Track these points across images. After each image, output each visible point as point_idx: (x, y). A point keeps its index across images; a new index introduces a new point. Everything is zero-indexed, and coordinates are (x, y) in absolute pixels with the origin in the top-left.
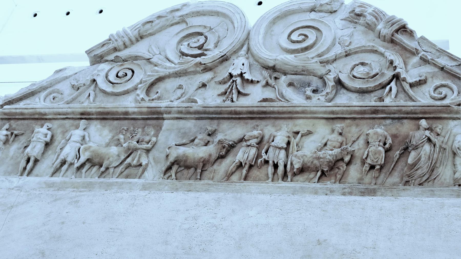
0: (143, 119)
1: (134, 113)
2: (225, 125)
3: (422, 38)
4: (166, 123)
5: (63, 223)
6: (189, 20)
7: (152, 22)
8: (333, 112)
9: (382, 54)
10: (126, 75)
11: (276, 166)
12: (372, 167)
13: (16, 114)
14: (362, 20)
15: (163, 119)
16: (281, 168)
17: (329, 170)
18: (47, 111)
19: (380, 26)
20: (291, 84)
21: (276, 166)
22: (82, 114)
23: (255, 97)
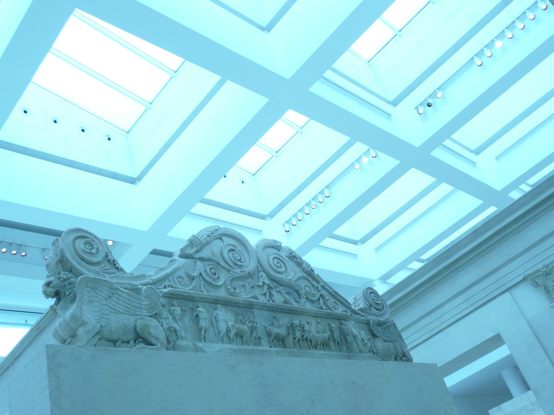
0: (244, 307)
1: (241, 303)
2: (279, 315)
3: (317, 275)
4: (256, 311)
5: (264, 377)
6: (224, 238)
7: (209, 236)
8: (316, 314)
9: (310, 281)
10: (215, 274)
11: (311, 341)
12: (338, 343)
13: (178, 295)
14: (294, 260)
15: (253, 308)
16: (313, 343)
17: (325, 345)
18: (197, 295)
19: (304, 266)
20: (288, 293)
21: (311, 341)
22: (215, 300)
23: (278, 299)
